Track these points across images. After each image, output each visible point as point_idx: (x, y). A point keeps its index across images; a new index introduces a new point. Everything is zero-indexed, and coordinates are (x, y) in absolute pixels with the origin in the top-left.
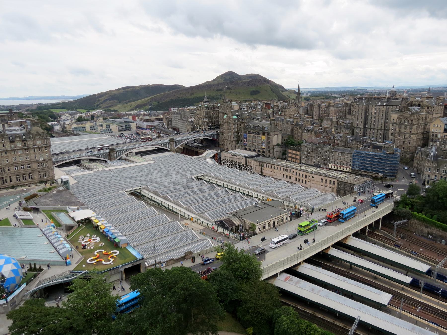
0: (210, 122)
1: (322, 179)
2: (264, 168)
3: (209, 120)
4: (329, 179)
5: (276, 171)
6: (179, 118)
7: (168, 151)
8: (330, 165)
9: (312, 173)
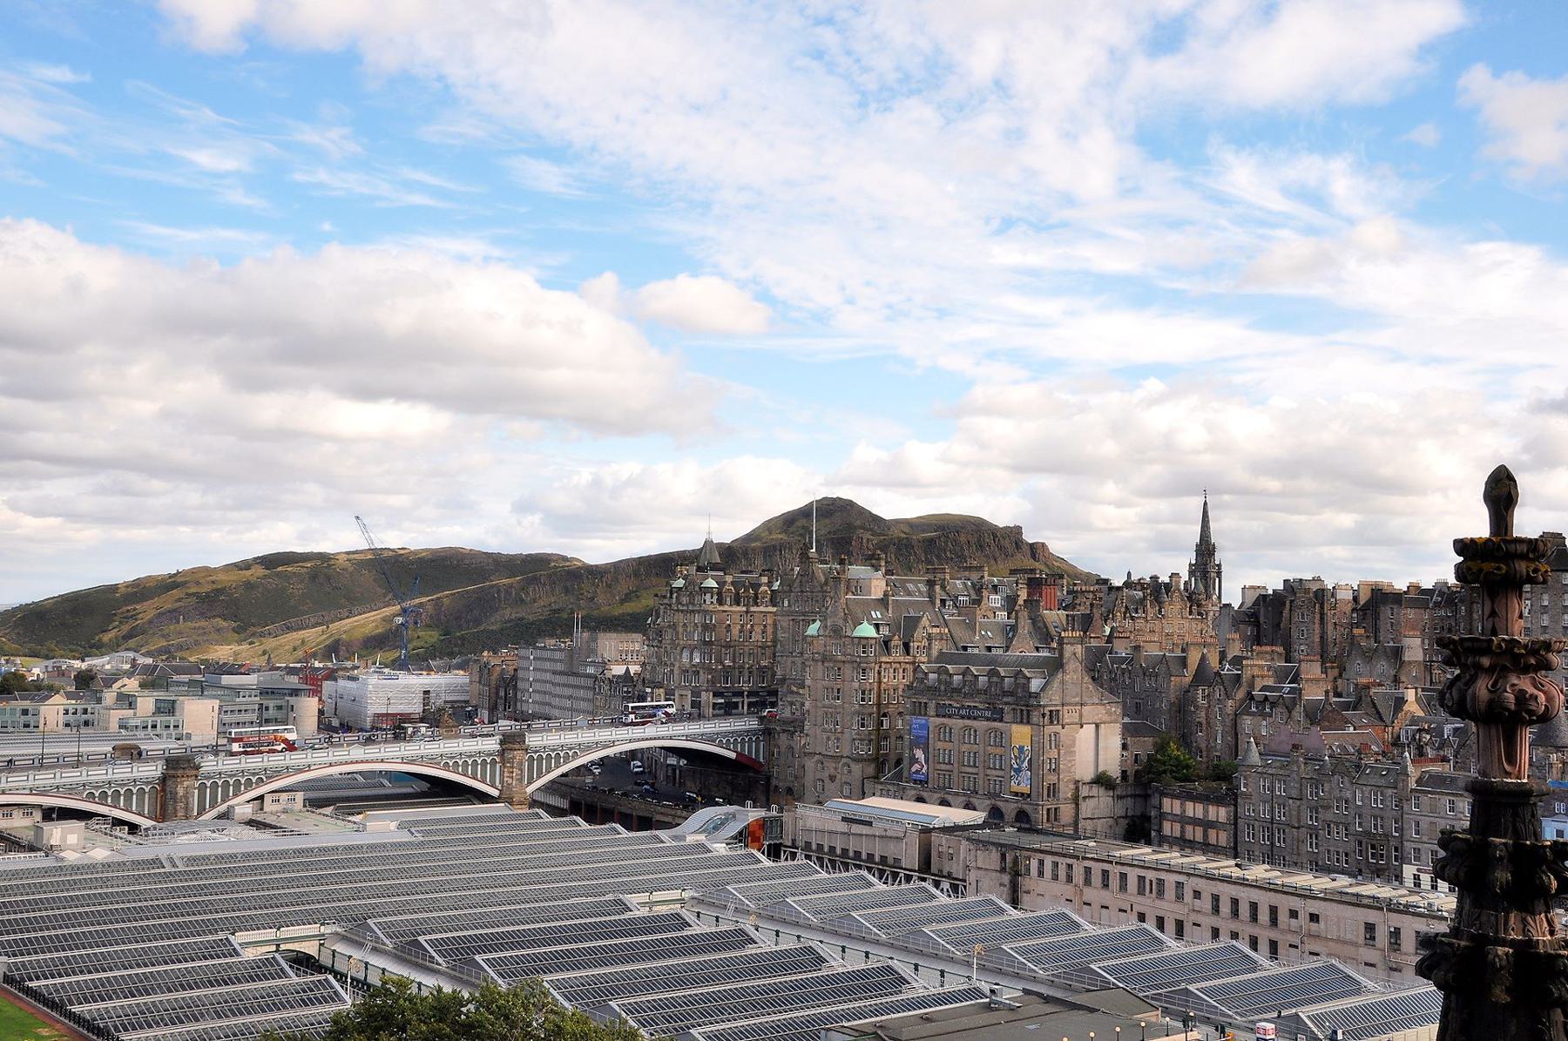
0: (727, 672)
1: (1370, 928)
5: (1094, 894)
6: (559, 667)
7: (484, 798)
8: (1409, 871)
9: (1306, 895)
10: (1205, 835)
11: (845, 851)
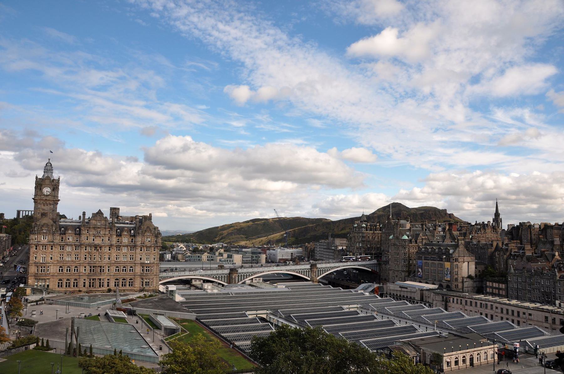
0: (368, 248)
1: (546, 318)
6: (325, 247)
7: (307, 280)
8: (557, 302)
9: (528, 308)
10: (499, 292)
11: (400, 295)
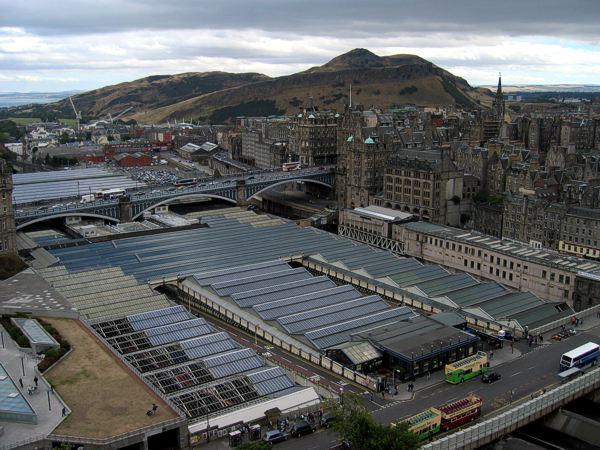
1: (544, 272)
2: (427, 245)
3: (316, 145)
4: (558, 273)
8: (561, 243)
